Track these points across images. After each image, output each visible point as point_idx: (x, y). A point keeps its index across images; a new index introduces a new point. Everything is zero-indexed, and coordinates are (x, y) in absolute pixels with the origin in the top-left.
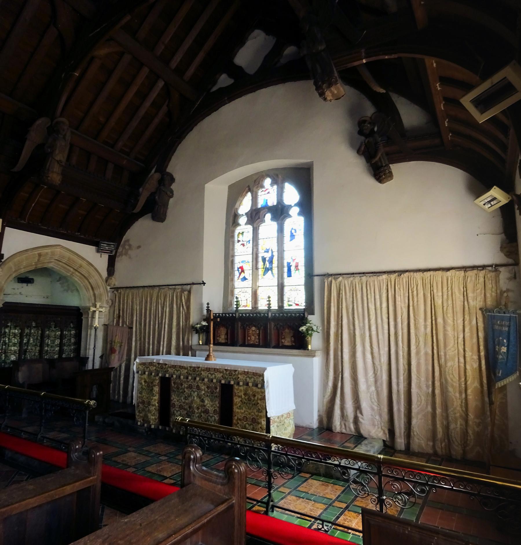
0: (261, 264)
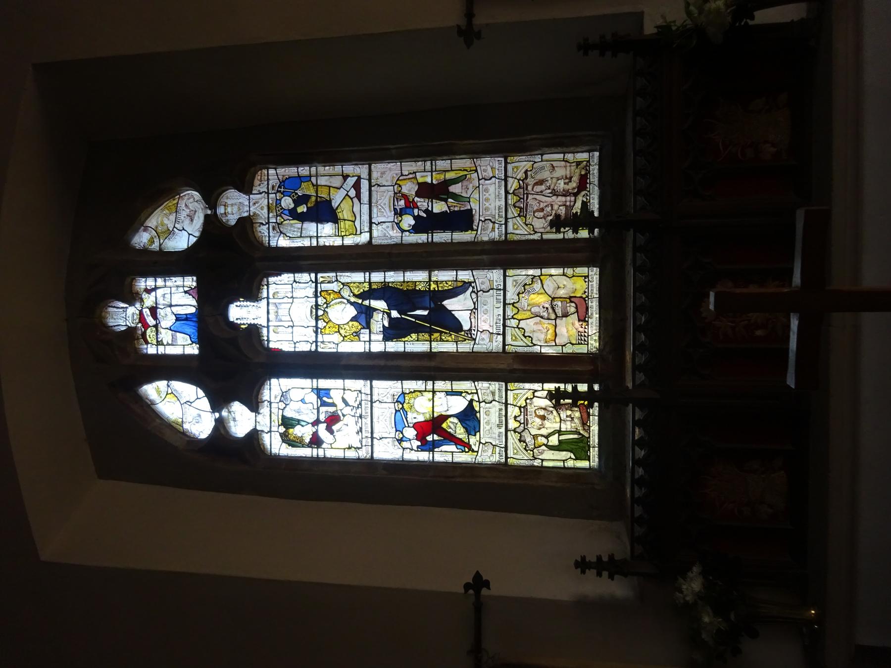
0: (415, 345)
